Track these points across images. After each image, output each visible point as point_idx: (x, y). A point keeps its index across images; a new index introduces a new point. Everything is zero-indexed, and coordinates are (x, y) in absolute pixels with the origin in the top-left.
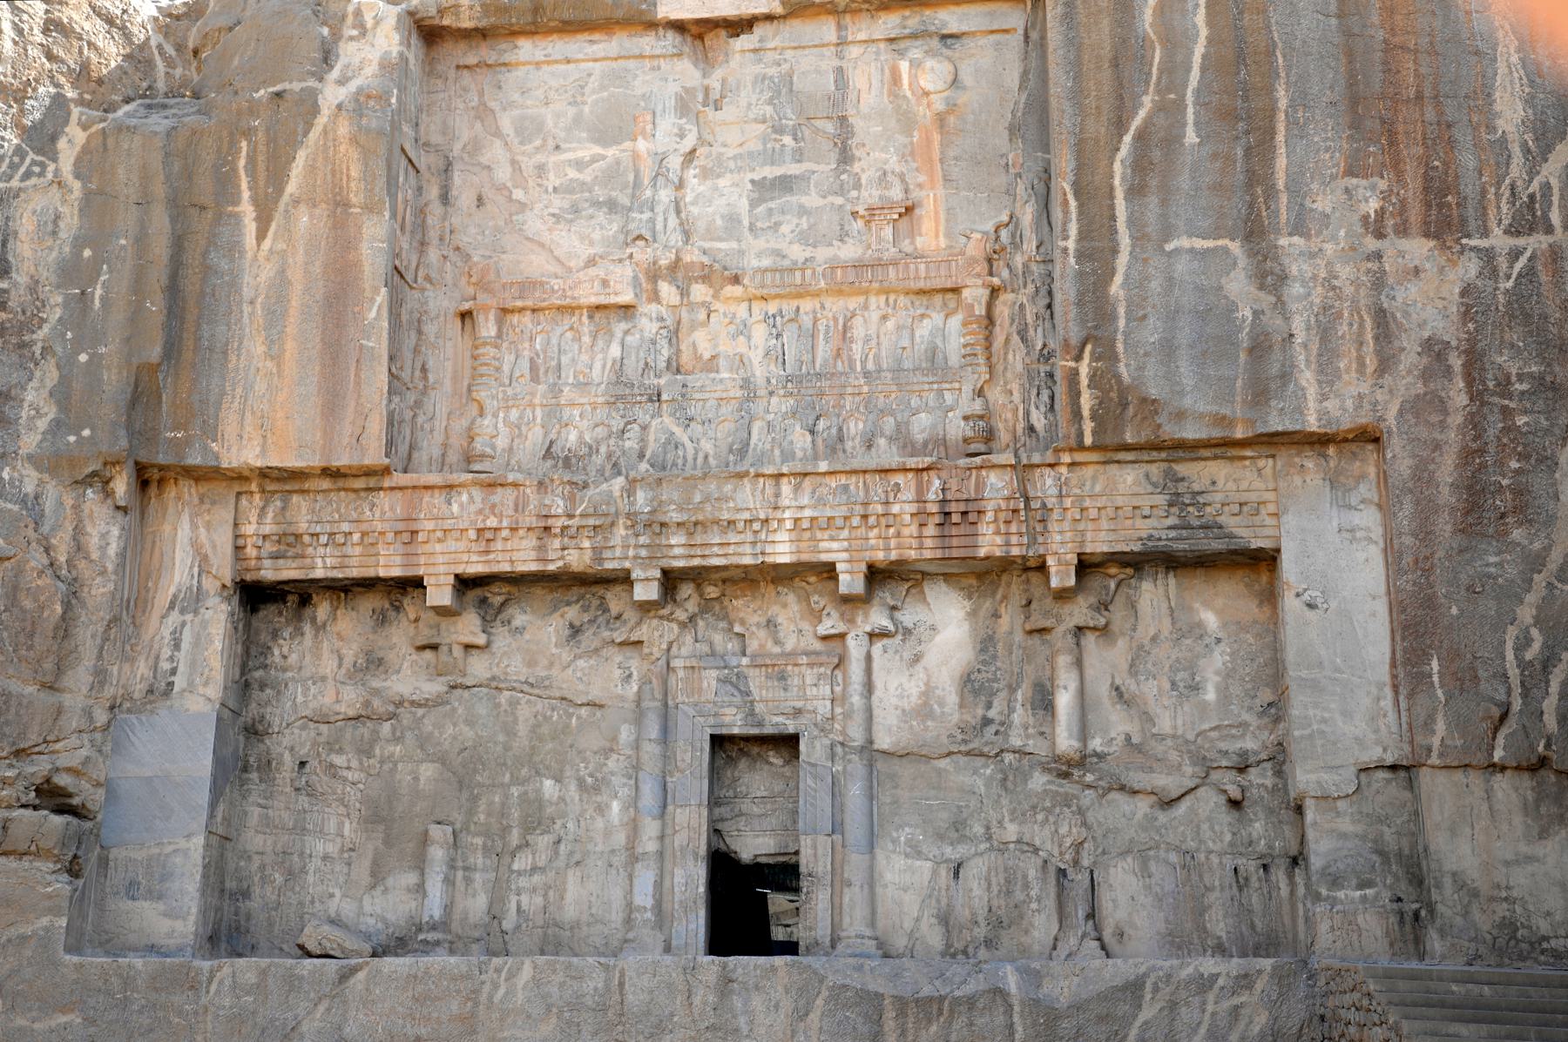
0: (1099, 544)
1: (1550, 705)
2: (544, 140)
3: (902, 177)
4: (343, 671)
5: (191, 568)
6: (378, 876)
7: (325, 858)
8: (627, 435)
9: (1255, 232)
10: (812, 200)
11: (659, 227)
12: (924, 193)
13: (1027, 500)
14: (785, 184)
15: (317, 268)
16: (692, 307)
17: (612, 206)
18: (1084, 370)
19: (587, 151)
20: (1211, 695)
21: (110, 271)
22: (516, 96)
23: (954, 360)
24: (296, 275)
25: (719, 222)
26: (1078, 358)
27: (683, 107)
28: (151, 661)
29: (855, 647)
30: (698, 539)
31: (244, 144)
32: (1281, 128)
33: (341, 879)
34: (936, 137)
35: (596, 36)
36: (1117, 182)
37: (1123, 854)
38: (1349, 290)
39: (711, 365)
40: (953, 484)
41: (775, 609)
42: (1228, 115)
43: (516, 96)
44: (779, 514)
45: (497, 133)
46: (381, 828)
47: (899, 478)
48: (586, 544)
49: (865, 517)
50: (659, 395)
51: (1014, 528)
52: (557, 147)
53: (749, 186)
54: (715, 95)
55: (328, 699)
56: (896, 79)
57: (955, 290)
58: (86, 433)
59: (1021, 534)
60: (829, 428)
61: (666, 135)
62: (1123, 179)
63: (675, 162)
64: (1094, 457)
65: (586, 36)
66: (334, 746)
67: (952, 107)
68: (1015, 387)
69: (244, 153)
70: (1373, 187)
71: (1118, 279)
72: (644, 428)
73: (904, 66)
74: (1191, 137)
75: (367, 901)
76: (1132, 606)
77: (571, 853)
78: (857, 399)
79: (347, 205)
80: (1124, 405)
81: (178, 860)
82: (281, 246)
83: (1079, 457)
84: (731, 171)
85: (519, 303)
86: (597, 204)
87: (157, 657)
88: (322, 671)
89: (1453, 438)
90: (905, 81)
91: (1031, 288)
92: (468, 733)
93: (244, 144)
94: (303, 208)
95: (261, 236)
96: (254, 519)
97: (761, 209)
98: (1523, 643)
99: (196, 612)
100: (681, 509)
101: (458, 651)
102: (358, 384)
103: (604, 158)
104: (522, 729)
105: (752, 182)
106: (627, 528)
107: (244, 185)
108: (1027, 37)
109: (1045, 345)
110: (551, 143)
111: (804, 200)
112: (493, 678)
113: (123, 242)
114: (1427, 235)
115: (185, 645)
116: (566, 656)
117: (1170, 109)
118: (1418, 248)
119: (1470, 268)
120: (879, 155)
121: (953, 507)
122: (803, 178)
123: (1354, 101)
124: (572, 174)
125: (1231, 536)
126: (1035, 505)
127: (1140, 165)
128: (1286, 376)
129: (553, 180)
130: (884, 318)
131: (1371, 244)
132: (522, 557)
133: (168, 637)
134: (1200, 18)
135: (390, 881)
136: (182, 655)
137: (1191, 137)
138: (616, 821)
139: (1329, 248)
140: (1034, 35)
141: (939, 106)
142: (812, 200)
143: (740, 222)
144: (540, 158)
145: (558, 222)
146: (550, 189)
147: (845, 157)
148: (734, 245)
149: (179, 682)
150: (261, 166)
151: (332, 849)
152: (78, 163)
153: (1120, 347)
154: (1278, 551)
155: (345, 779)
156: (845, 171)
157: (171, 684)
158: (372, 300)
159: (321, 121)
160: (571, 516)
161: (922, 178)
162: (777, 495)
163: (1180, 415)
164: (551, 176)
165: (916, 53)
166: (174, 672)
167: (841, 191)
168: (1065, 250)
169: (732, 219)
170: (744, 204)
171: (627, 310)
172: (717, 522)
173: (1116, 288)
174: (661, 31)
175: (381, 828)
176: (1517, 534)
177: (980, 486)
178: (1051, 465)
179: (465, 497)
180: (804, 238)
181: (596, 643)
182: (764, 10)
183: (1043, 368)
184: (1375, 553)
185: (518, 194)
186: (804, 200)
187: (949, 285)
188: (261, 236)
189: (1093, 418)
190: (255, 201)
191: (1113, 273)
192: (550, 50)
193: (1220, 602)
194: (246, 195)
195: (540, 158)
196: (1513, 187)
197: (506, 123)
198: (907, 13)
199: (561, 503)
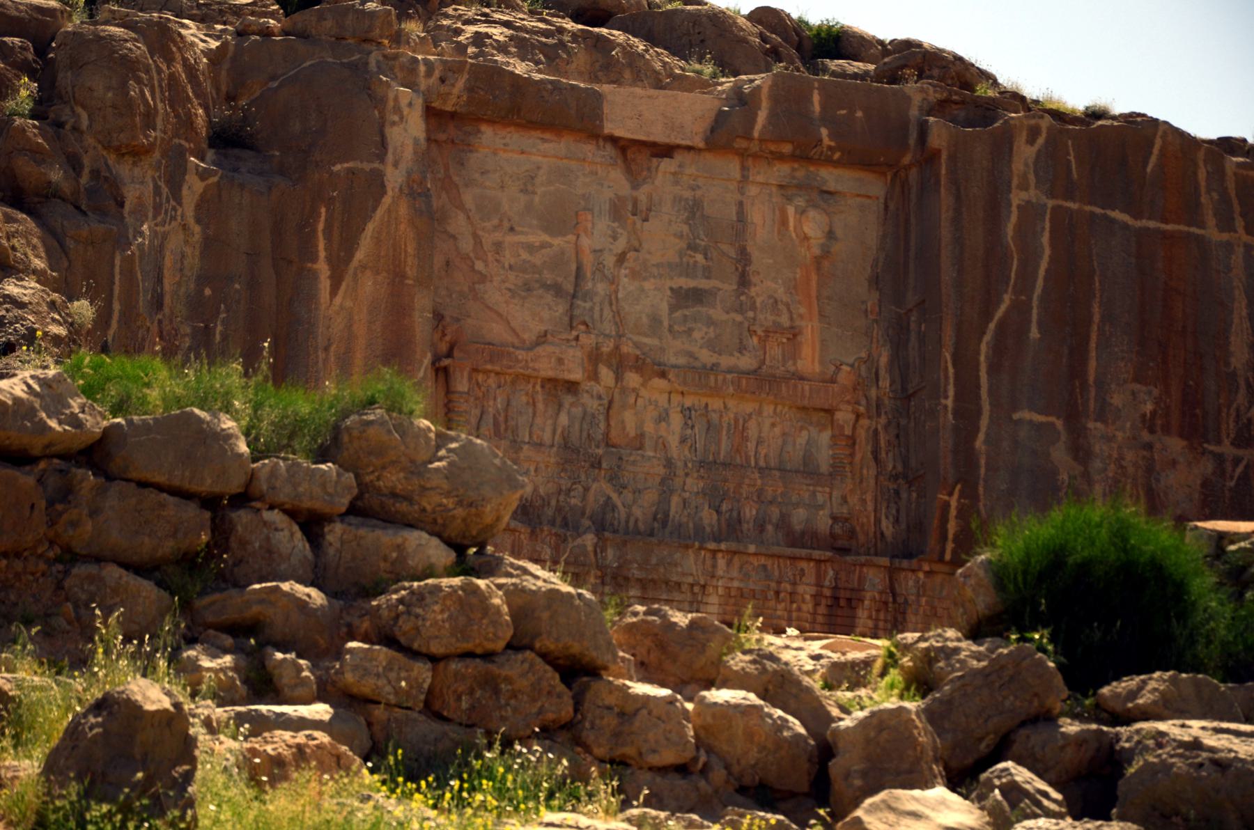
2: (501, 220)
3: (788, 306)
8: (572, 494)
9: (1073, 417)
10: (717, 313)
11: (597, 315)
12: (803, 323)
13: (894, 595)
14: (697, 296)
16: (624, 391)
17: (557, 290)
18: (954, 503)
21: (227, 311)
25: (645, 320)
26: (951, 494)
27: (616, 211)
31: (323, 210)
32: (1094, 336)
34: (814, 277)
36: (982, 358)
38: (1131, 470)
39: (638, 442)
40: (843, 575)
43: (477, 176)
44: (714, 582)
45: (461, 207)
47: (804, 565)
49: (777, 593)
50: (600, 463)
51: (882, 616)
53: (669, 293)
54: (643, 206)
56: (784, 222)
57: (830, 412)
59: (886, 621)
60: (731, 510)
62: (987, 357)
63: (610, 260)
65: (538, 134)
67: (826, 253)
70: (1150, 393)
71: (981, 436)
72: (587, 489)
73: (791, 210)
74: (1034, 333)
78: (752, 489)
79: (404, 276)
82: (349, 304)
83: (937, 567)
84: (654, 277)
85: (489, 367)
86: (547, 287)
90: (791, 224)
91: (883, 420)
93: (323, 210)
94: (368, 273)
95: (334, 292)
97: (678, 314)
100: (640, 568)
105: (671, 289)
106: (596, 577)
107: (321, 245)
108: (886, 207)
109: (894, 467)
110: (506, 225)
111: (711, 312)
114: (1181, 436)
117: (1021, 309)
118: (1176, 444)
119: (1208, 466)
121: (842, 594)
122: (712, 293)
124: (525, 255)
127: (998, 349)
130: (773, 425)
131: (1146, 436)
134: (1045, 239)
137: (1034, 333)
139: (1120, 435)
141: (817, 251)
142: (717, 313)
143: (661, 322)
145: (513, 297)
146: (507, 265)
147: (744, 281)
148: (656, 342)
153: (981, 490)
156: (743, 293)
161: (802, 310)
162: (714, 566)
164: (507, 253)
165: (800, 202)
167: (740, 309)
168: (946, 407)
170: (664, 307)
173: (979, 443)
174: (601, 143)
177: (861, 579)
178: (913, 571)
180: (711, 345)
185: (479, 266)
187: (826, 407)
188: (334, 292)
189: (954, 541)
190: (329, 260)
191: (977, 430)
194: (322, 254)
195: (498, 236)
196: (1238, 410)
197: (468, 198)
198: (796, 166)
199: (549, 551)
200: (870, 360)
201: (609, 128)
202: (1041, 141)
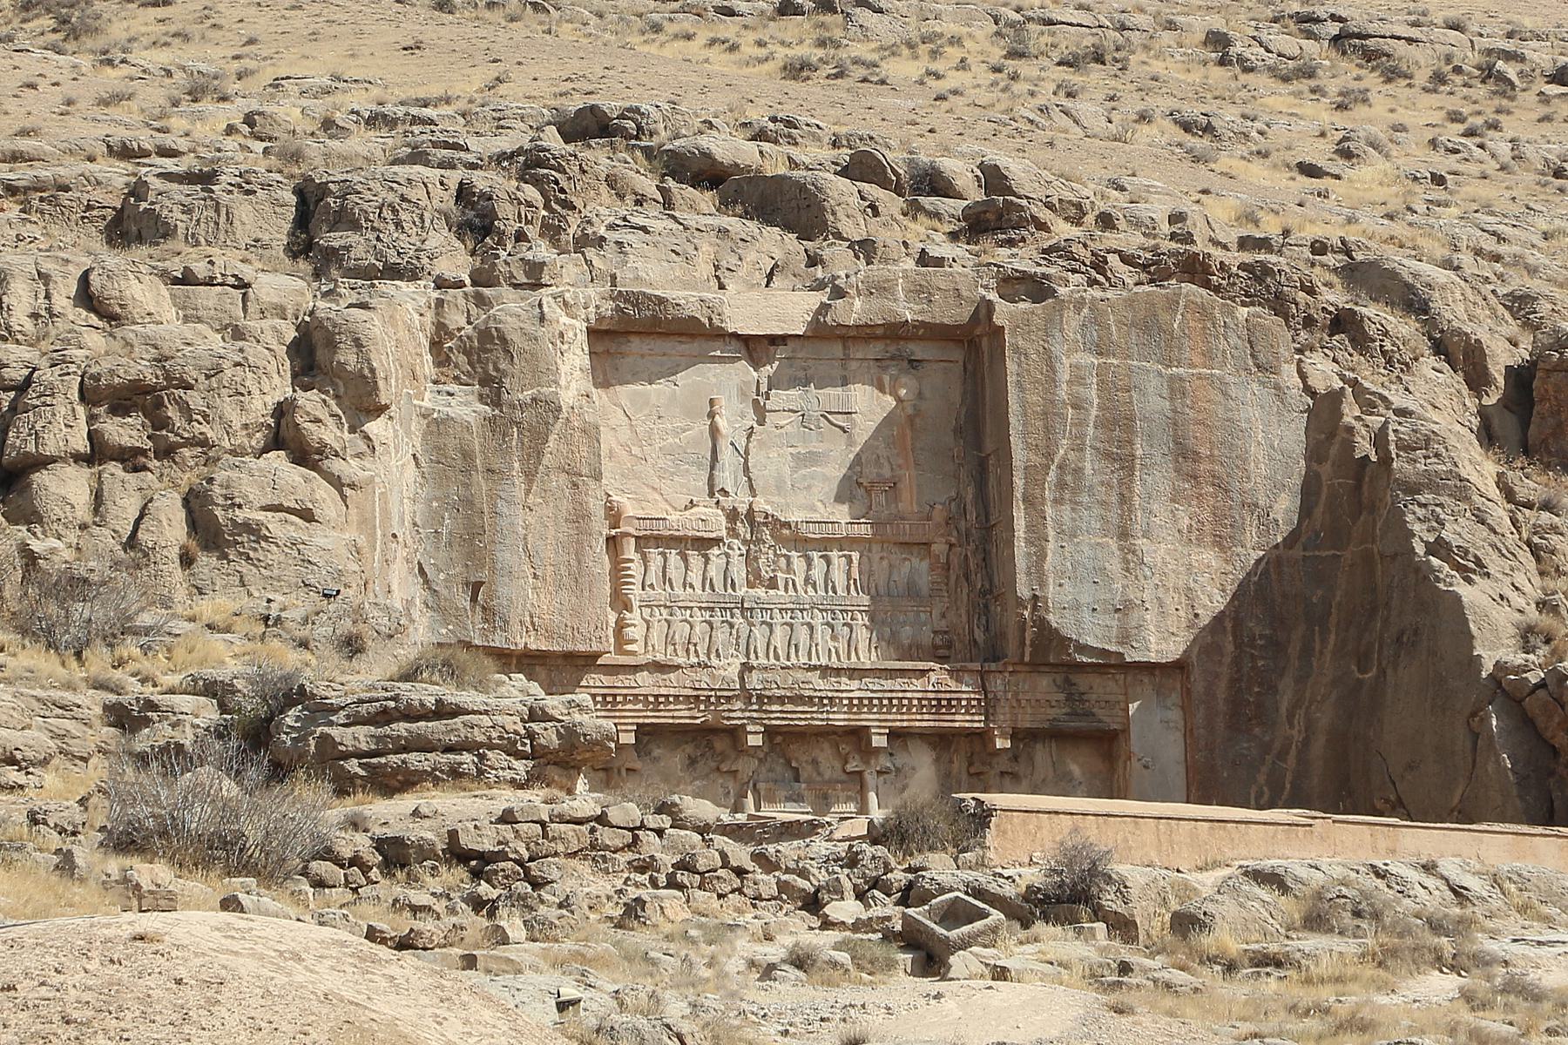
0: (1026, 723)
9: (1124, 534)
23: (925, 591)
29: (870, 779)
41: (816, 753)
42: (1108, 456)
57: (928, 544)
64: (1027, 668)
68: (963, 611)
76: (1031, 759)
83: (1018, 668)
89: (1225, 671)
95: (528, 492)
101: (624, 772)
126: (990, 696)
127: (1061, 485)
132: (682, 715)
140: (969, 367)
141: (910, 411)
154: (1126, 731)
161: (901, 461)
163: (1083, 649)
170: (787, 470)
171: (717, 541)
172: (802, 697)
176: (1257, 730)
183: (981, 601)
184: (1179, 736)
185: (635, 450)
188: (528, 492)
200: (959, 498)
201: (731, 328)
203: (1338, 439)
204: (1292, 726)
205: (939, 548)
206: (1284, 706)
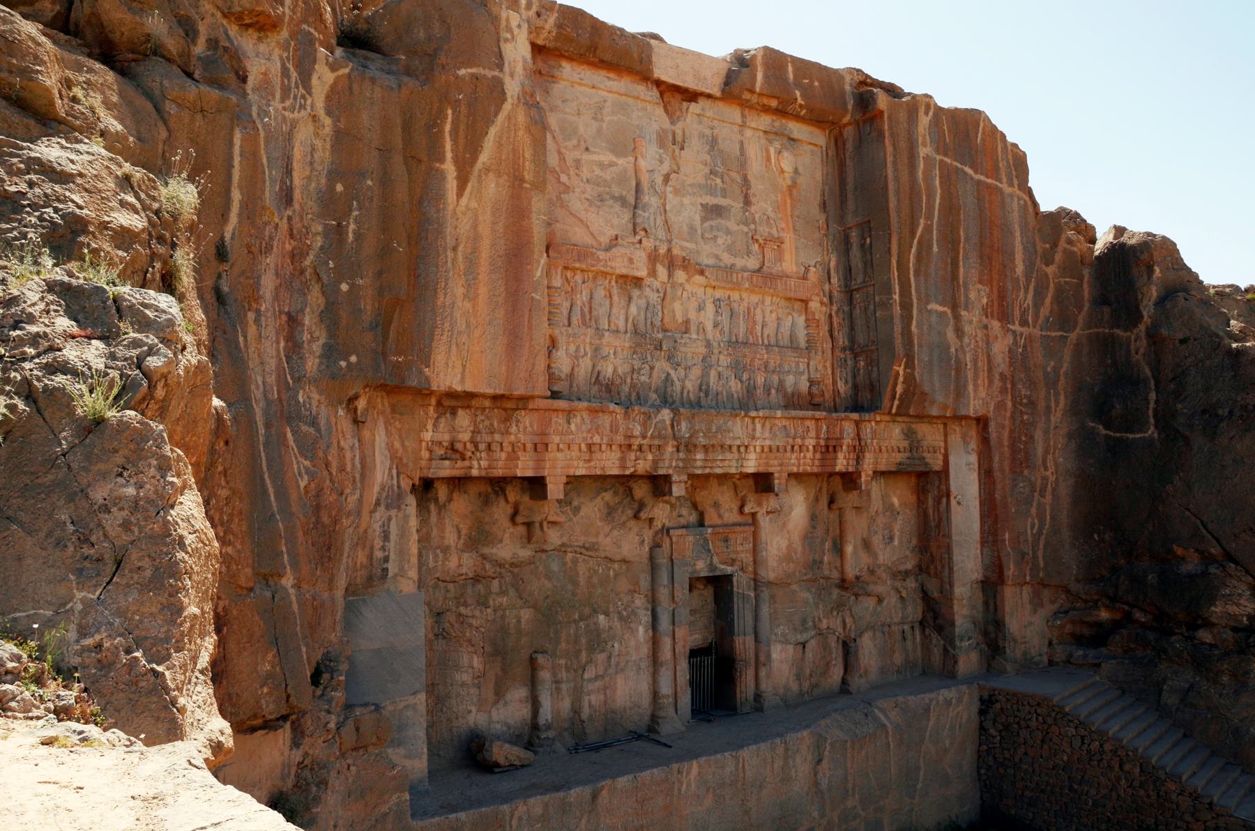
1: (1040, 554)
4: (462, 541)
5: (390, 469)
6: (499, 693)
7: (463, 684)
10: (732, 225)
15: (500, 228)
17: (622, 200)
19: (607, 157)
20: (896, 543)
21: (360, 209)
22: (559, 103)
24: (485, 230)
25: (685, 228)
27: (661, 143)
28: (367, 551)
30: (711, 456)
31: (450, 112)
33: (475, 699)
34: (789, 201)
35: (612, 75)
37: (866, 630)
44: (754, 443)
46: (499, 659)
47: (808, 423)
48: (650, 457)
52: (587, 149)
54: (679, 138)
55: (453, 563)
56: (768, 159)
58: (353, 359)
61: (650, 159)
63: (659, 180)
66: (460, 600)
67: (794, 185)
68: (828, 364)
69: (450, 117)
71: (914, 322)
72: (652, 368)
73: (772, 151)
74: (935, 249)
75: (494, 713)
77: (618, 663)
79: (522, 180)
80: (914, 394)
81: (410, 713)
82: (474, 204)
85: (577, 265)
87: (372, 548)
88: (446, 542)
91: (835, 308)
92: (548, 585)
93: (450, 112)
94: (491, 175)
96: (430, 427)
97: (707, 224)
98: (1033, 526)
99: (399, 508)
100: (705, 436)
102: (530, 328)
103: (616, 165)
104: (582, 580)
110: (583, 145)
111: (728, 224)
112: (563, 545)
113: (369, 183)
114: (999, 320)
115: (393, 537)
116: (607, 528)
117: (928, 229)
120: (763, 206)
123: (982, 244)
124: (598, 172)
125: (927, 464)
127: (919, 258)
128: (965, 386)
129: (585, 173)
133: (378, 530)
135: (509, 696)
136: (391, 545)
137: (935, 249)
138: (642, 640)
141: (789, 182)
142: (732, 225)
144: (577, 154)
145: (591, 205)
147: (747, 202)
149: (392, 568)
150: (462, 134)
151: (466, 677)
152: (328, 98)
155: (471, 625)
157: (385, 570)
158: (538, 262)
159: (507, 107)
160: (644, 437)
161: (783, 225)
162: (754, 430)
165: (777, 145)
166: (386, 559)
167: (746, 223)
169: (692, 228)
170: (697, 218)
173: (914, 328)
175: (499, 659)
177: (842, 431)
179: (578, 419)
180: (730, 249)
181: (624, 518)
182: (708, 91)
183: (842, 356)
185: (564, 178)
186: (728, 224)
190: (456, 160)
192: (582, 76)
193: (898, 492)
194: (449, 155)
195: (577, 154)
202: (931, 114)
203: (1060, 249)
204: (1046, 469)
205: (814, 305)
206: (1040, 451)
